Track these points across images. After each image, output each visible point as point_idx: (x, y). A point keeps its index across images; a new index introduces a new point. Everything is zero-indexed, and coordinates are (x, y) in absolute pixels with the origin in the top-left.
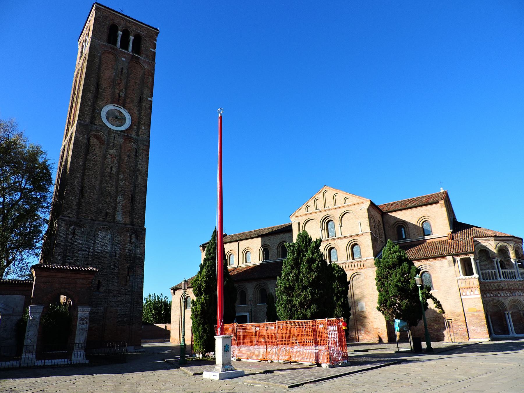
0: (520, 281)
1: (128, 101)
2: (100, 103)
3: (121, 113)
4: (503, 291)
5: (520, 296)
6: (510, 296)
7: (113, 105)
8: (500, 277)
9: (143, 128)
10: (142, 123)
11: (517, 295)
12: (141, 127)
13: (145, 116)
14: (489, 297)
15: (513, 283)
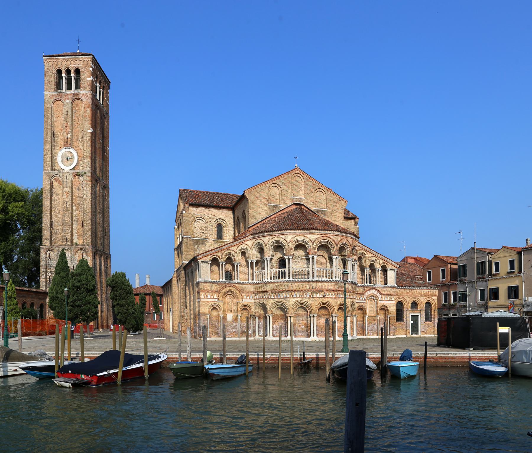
0: (287, 282)
1: (74, 140)
2: (56, 149)
3: (71, 152)
4: (267, 293)
5: (285, 298)
6: (274, 298)
7: (64, 148)
8: (267, 279)
9: (86, 161)
10: (85, 156)
11: (282, 297)
12: (84, 161)
13: (86, 149)
14: (258, 299)
15: (279, 284)
